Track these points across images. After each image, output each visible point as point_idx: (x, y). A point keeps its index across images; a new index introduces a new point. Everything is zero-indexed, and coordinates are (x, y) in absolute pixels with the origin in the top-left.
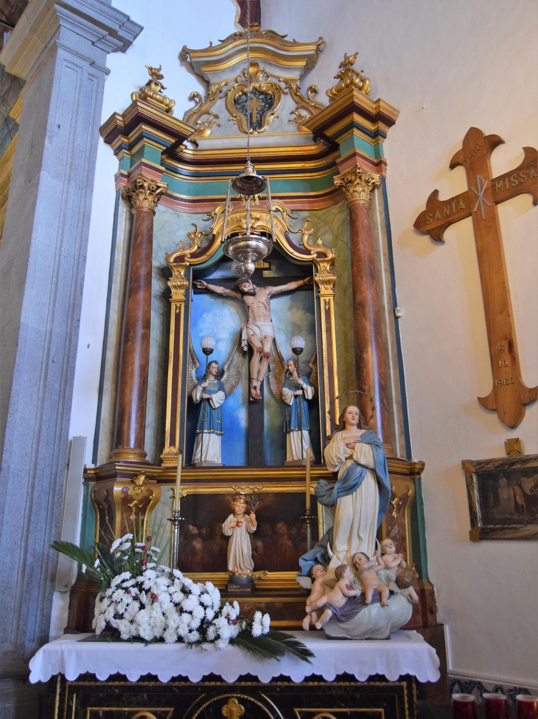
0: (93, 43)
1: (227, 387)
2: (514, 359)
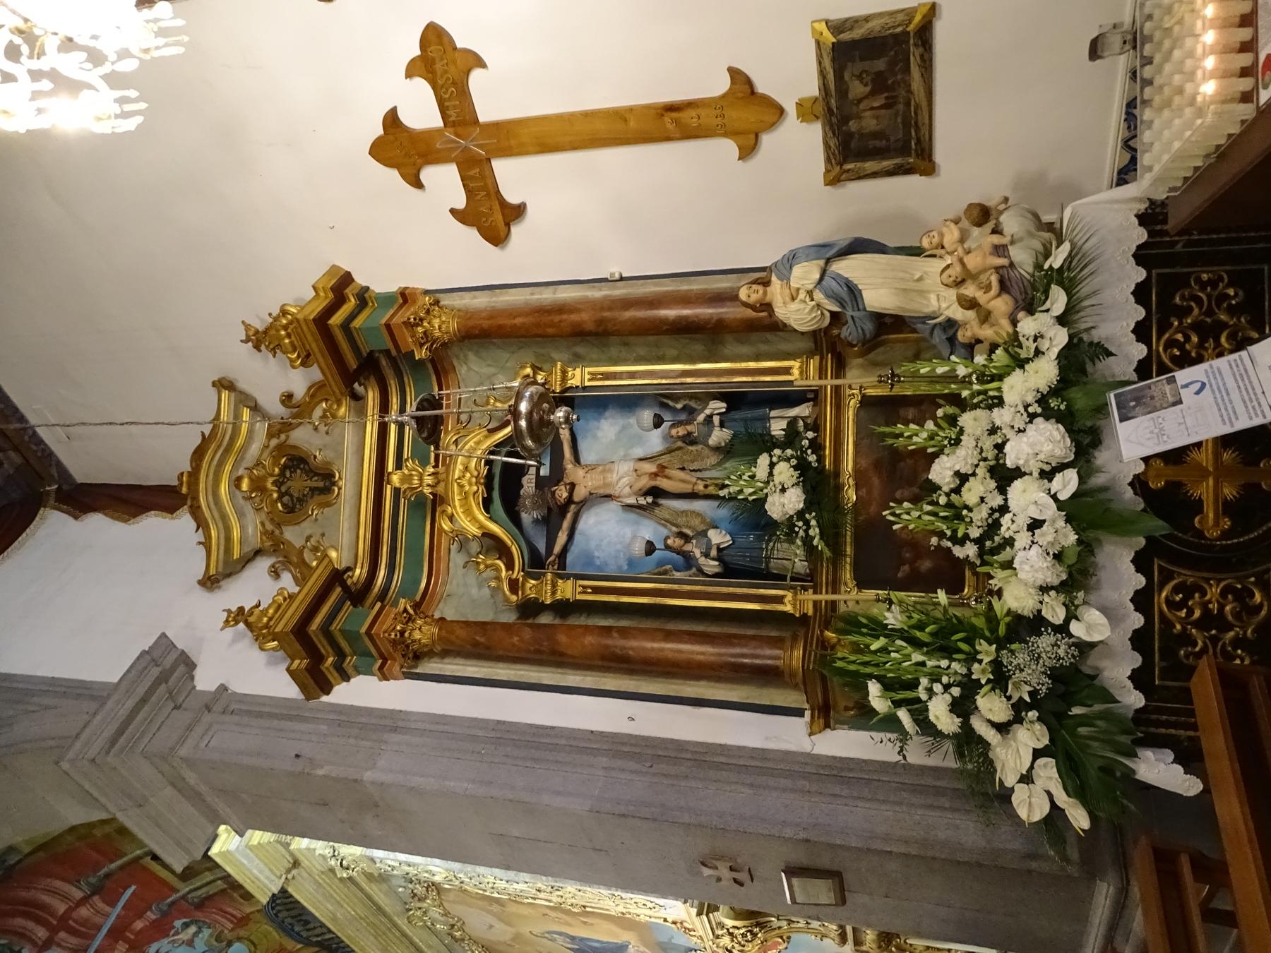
0: (176, 707)
1: (702, 527)
2: (690, 105)
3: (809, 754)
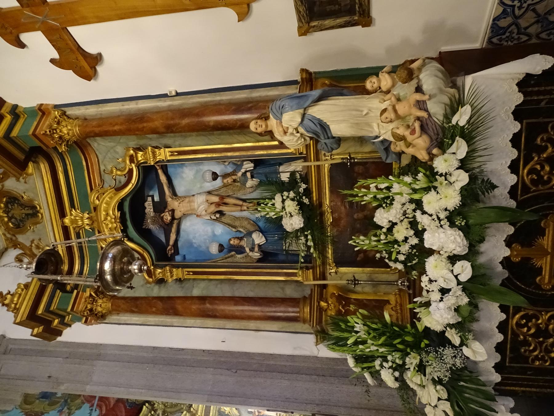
3: (317, 357)
